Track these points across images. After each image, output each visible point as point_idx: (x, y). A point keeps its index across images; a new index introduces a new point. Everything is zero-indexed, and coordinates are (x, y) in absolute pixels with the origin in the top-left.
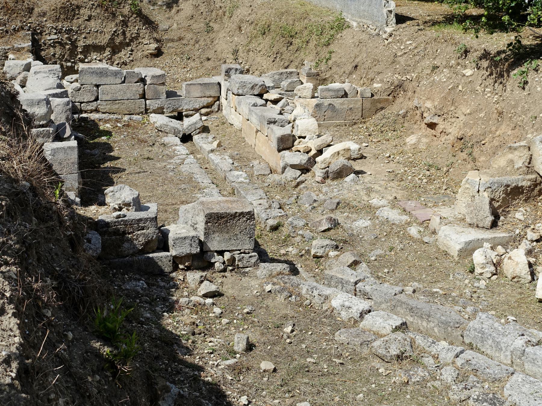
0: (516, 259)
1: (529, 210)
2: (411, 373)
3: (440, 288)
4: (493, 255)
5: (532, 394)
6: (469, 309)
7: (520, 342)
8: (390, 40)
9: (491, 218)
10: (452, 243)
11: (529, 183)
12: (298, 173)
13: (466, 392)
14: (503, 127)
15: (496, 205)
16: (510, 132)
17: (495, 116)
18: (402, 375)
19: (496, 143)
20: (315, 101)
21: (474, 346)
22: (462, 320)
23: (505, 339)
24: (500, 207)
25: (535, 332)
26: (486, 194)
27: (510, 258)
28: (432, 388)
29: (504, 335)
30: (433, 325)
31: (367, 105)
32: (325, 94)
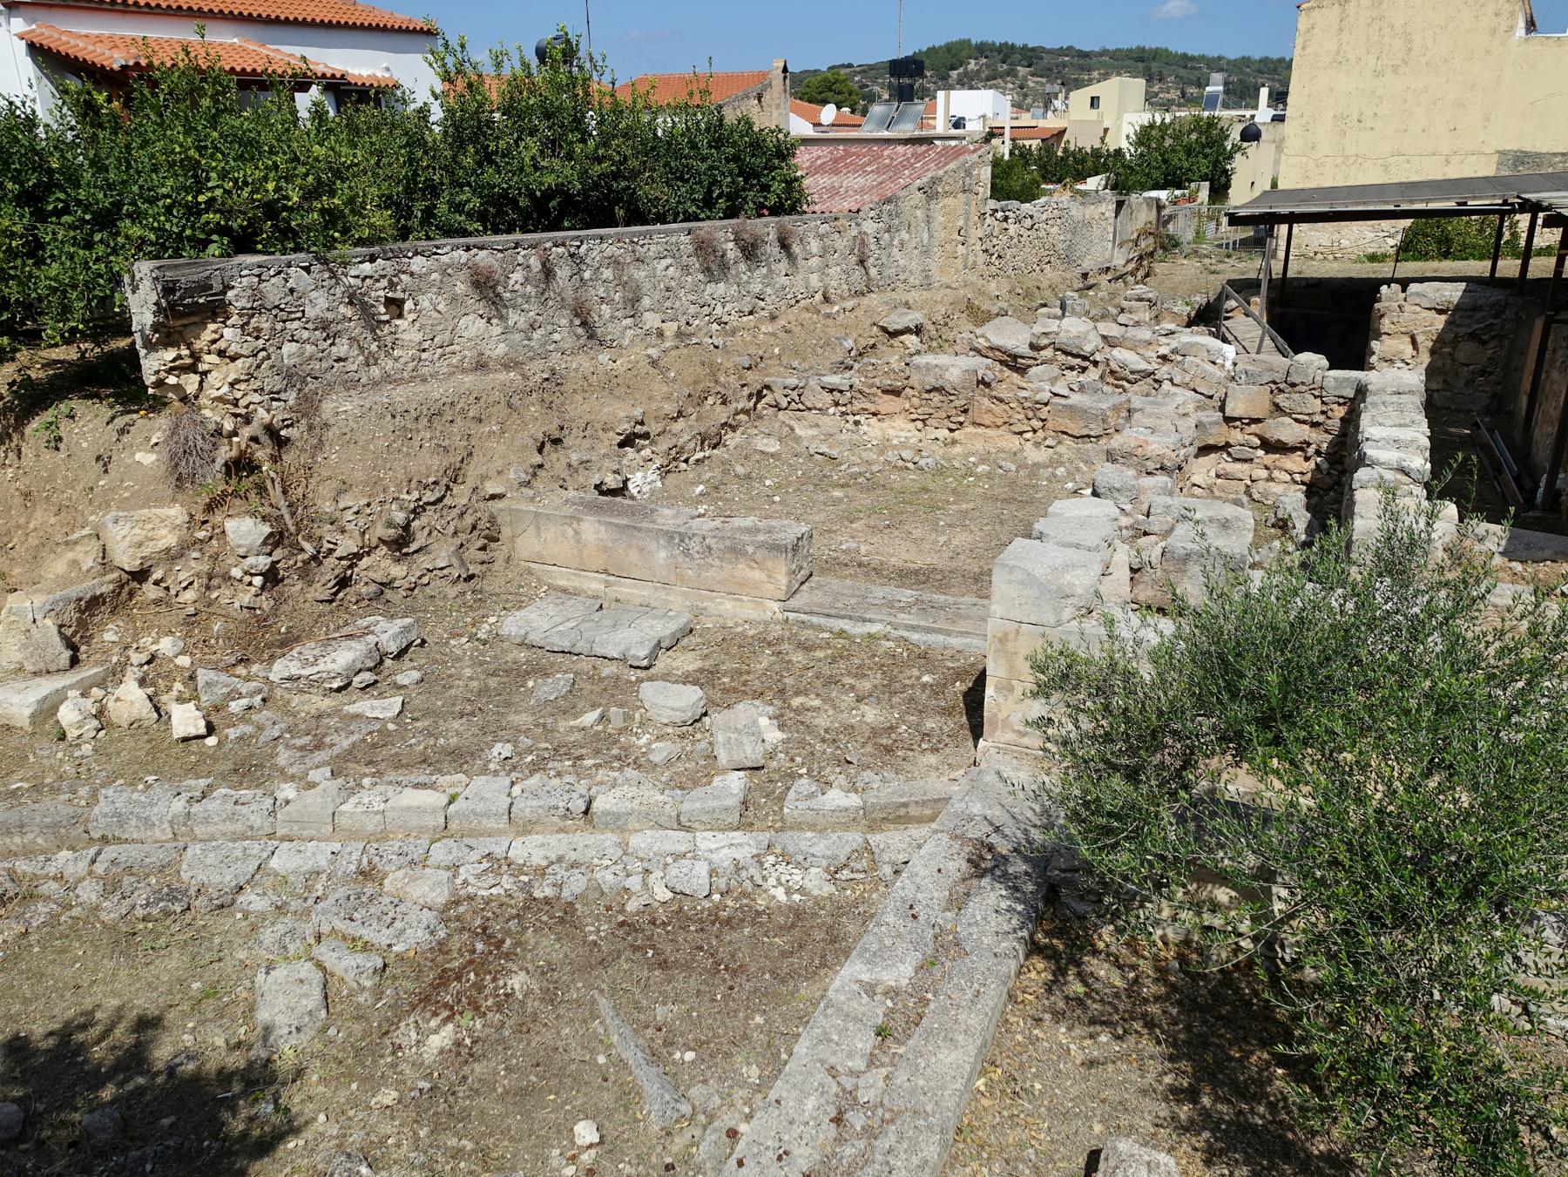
0: (129, 698)
1: (121, 624)
2: (28, 915)
3: (21, 780)
4: (90, 706)
5: (222, 862)
6: (83, 791)
7: (179, 805)
9: (68, 654)
10: (14, 710)
11: (111, 587)
13: (127, 902)
14: (39, 514)
15: (69, 632)
16: (53, 520)
17: (18, 500)
18: (14, 926)
19: (33, 541)
21: (110, 836)
22: (80, 811)
23: (156, 810)
24: (74, 635)
25: (192, 782)
26: (48, 622)
27: (118, 699)
28: (70, 922)
29: (151, 805)
30: (33, 836)
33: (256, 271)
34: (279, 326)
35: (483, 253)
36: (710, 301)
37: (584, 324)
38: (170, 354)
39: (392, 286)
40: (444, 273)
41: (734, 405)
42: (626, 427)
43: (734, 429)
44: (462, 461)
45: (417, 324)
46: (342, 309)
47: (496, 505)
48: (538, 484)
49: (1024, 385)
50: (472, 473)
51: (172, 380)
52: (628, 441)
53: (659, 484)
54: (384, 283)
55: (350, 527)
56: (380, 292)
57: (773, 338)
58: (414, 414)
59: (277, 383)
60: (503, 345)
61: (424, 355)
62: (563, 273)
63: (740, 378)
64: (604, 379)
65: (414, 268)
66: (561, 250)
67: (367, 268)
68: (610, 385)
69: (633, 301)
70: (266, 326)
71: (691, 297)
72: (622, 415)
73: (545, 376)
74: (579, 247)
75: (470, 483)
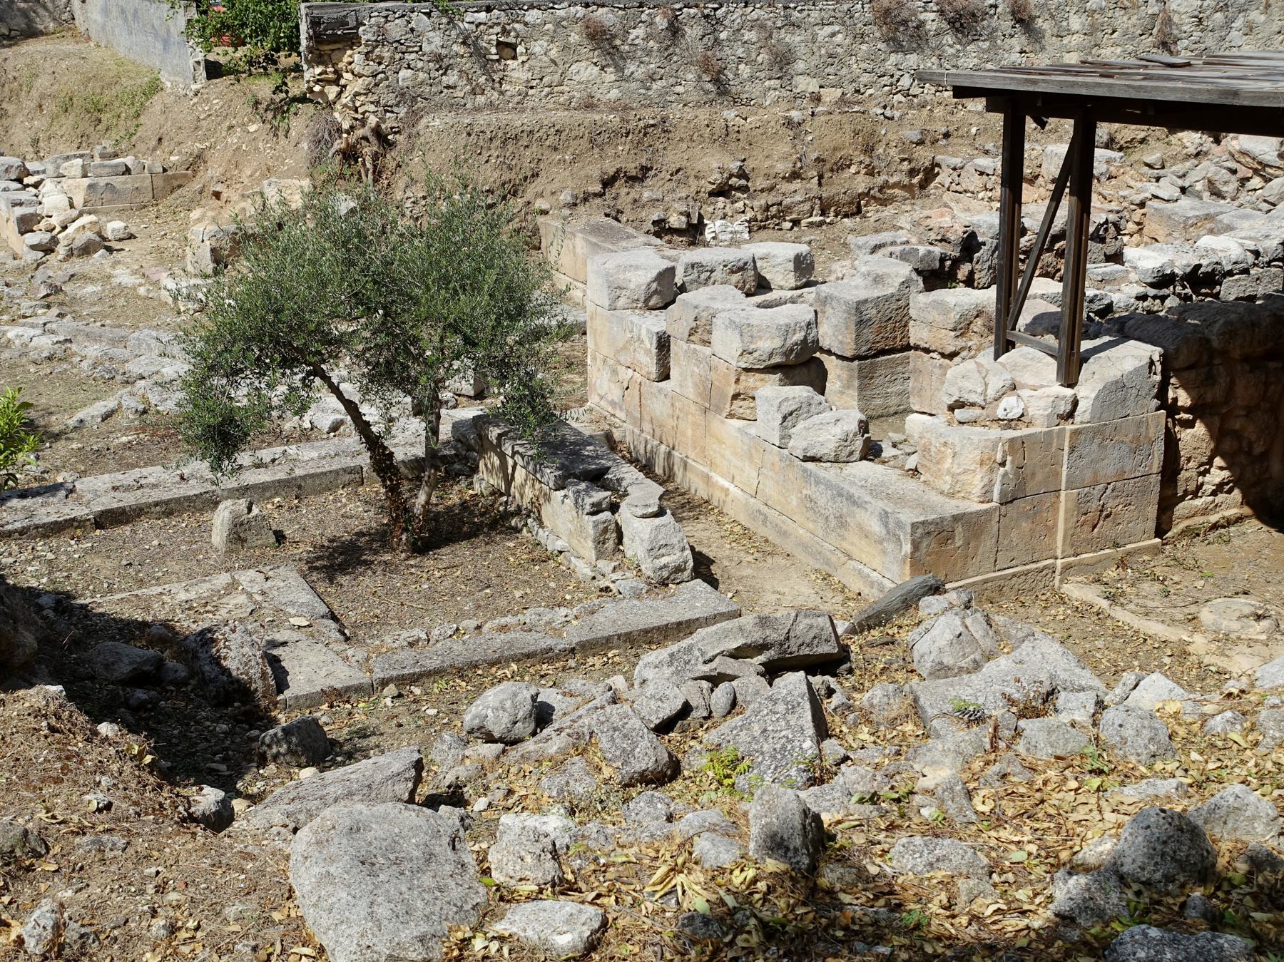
8: (195, 100)
12: (41, 254)
20: (86, 181)
26: (208, 243)
31: (159, 182)
32: (99, 171)
33: (384, 14)
34: (398, 56)
35: (600, 10)
36: (892, 70)
37: (716, 81)
38: (318, 70)
39: (505, 32)
40: (558, 24)
41: (883, 178)
42: (716, 177)
43: (884, 202)
44: (526, 178)
45: (527, 66)
46: (455, 47)
47: (541, 220)
48: (582, 209)
49: (1132, 183)
50: (531, 190)
51: (317, 88)
52: (722, 191)
53: (746, 236)
54: (498, 29)
55: (408, 213)
56: (493, 36)
57: (977, 117)
58: (488, 135)
59: (390, 99)
60: (616, 91)
61: (531, 92)
62: (692, 32)
63: (903, 151)
64: (717, 131)
65: (527, 19)
66: (692, 11)
67: (482, 16)
68: (726, 136)
69: (782, 62)
70: (387, 55)
71: (864, 66)
72: (715, 165)
73: (652, 122)
74: (716, 9)
75: (525, 199)
